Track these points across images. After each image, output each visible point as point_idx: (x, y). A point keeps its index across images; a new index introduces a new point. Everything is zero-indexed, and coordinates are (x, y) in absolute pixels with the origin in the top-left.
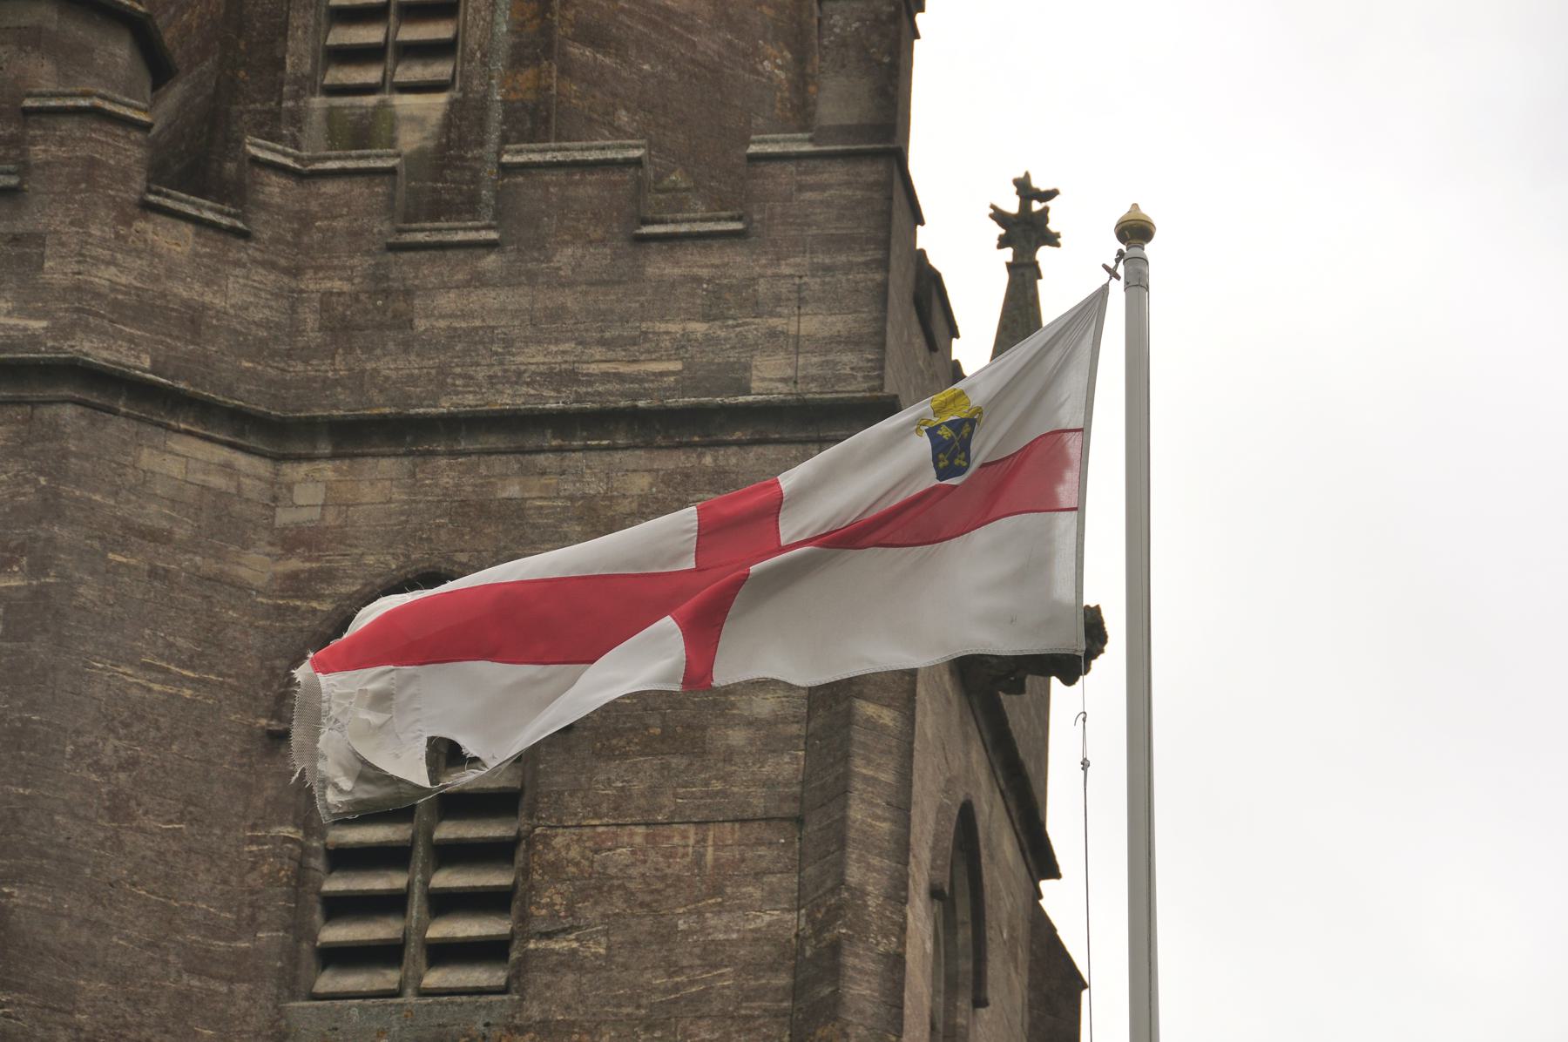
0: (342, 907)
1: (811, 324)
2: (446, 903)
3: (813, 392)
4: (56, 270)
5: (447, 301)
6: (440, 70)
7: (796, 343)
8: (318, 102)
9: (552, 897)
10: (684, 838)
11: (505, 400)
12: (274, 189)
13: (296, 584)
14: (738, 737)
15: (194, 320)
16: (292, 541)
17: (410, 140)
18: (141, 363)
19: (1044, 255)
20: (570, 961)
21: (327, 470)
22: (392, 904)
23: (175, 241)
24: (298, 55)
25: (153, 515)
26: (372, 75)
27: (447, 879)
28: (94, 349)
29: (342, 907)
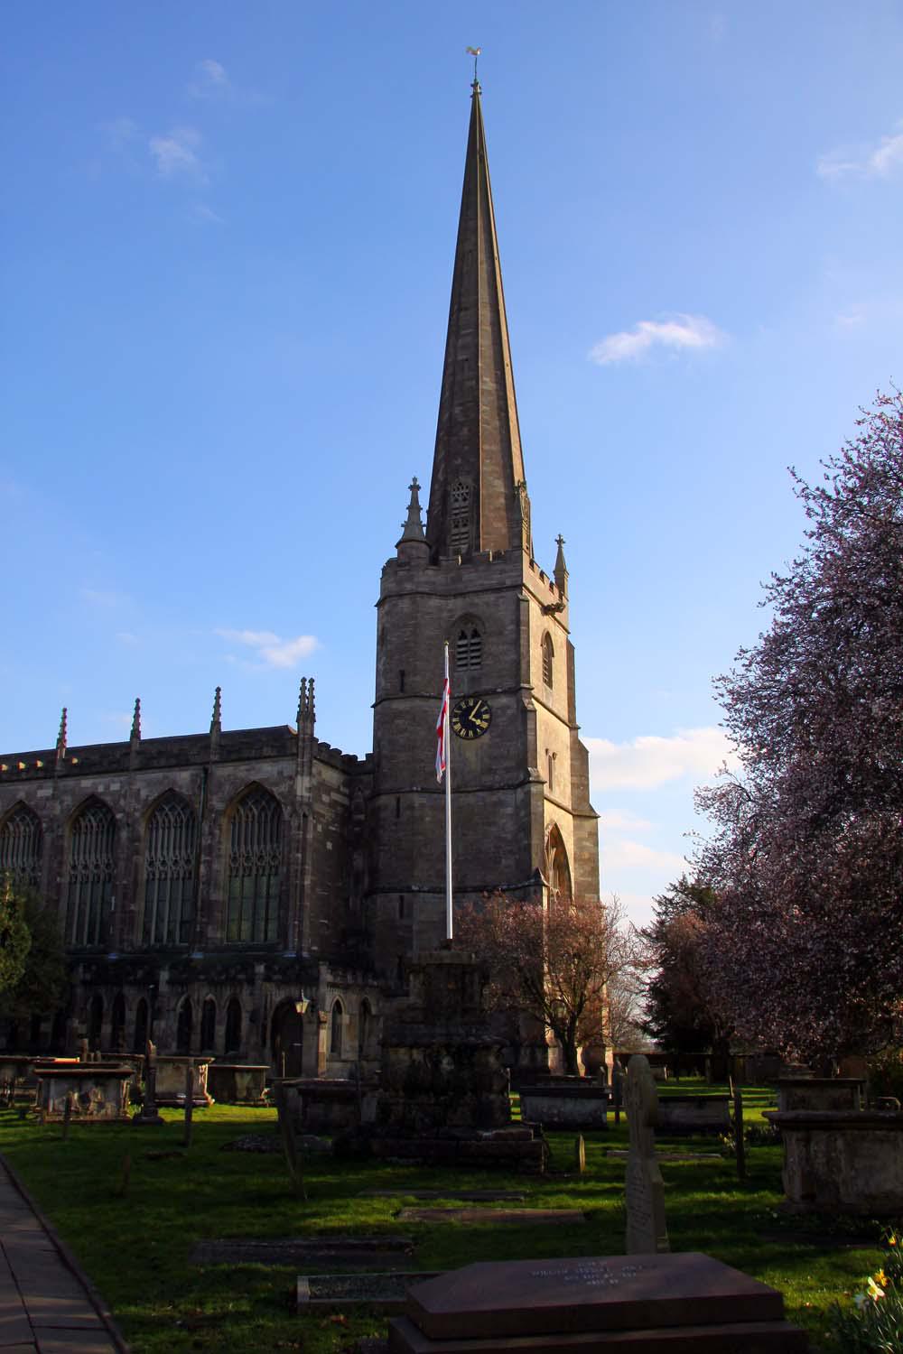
0: (460, 659)
1: (514, 574)
2: (472, 658)
3: (515, 584)
4: (416, 580)
5: (466, 576)
6: (466, 541)
7: (510, 577)
8: (451, 547)
9: (485, 656)
10: (501, 647)
11: (475, 589)
12: (444, 563)
13: (451, 617)
14: (506, 632)
15: (434, 583)
16: (450, 611)
17: (463, 551)
18: (427, 590)
19: (563, 545)
20: (488, 665)
21: (453, 601)
22: (466, 658)
23: (430, 572)
24: (448, 541)
25: (430, 611)
26: (457, 543)
27: (473, 654)
28: (420, 589)
29: (460, 659)
